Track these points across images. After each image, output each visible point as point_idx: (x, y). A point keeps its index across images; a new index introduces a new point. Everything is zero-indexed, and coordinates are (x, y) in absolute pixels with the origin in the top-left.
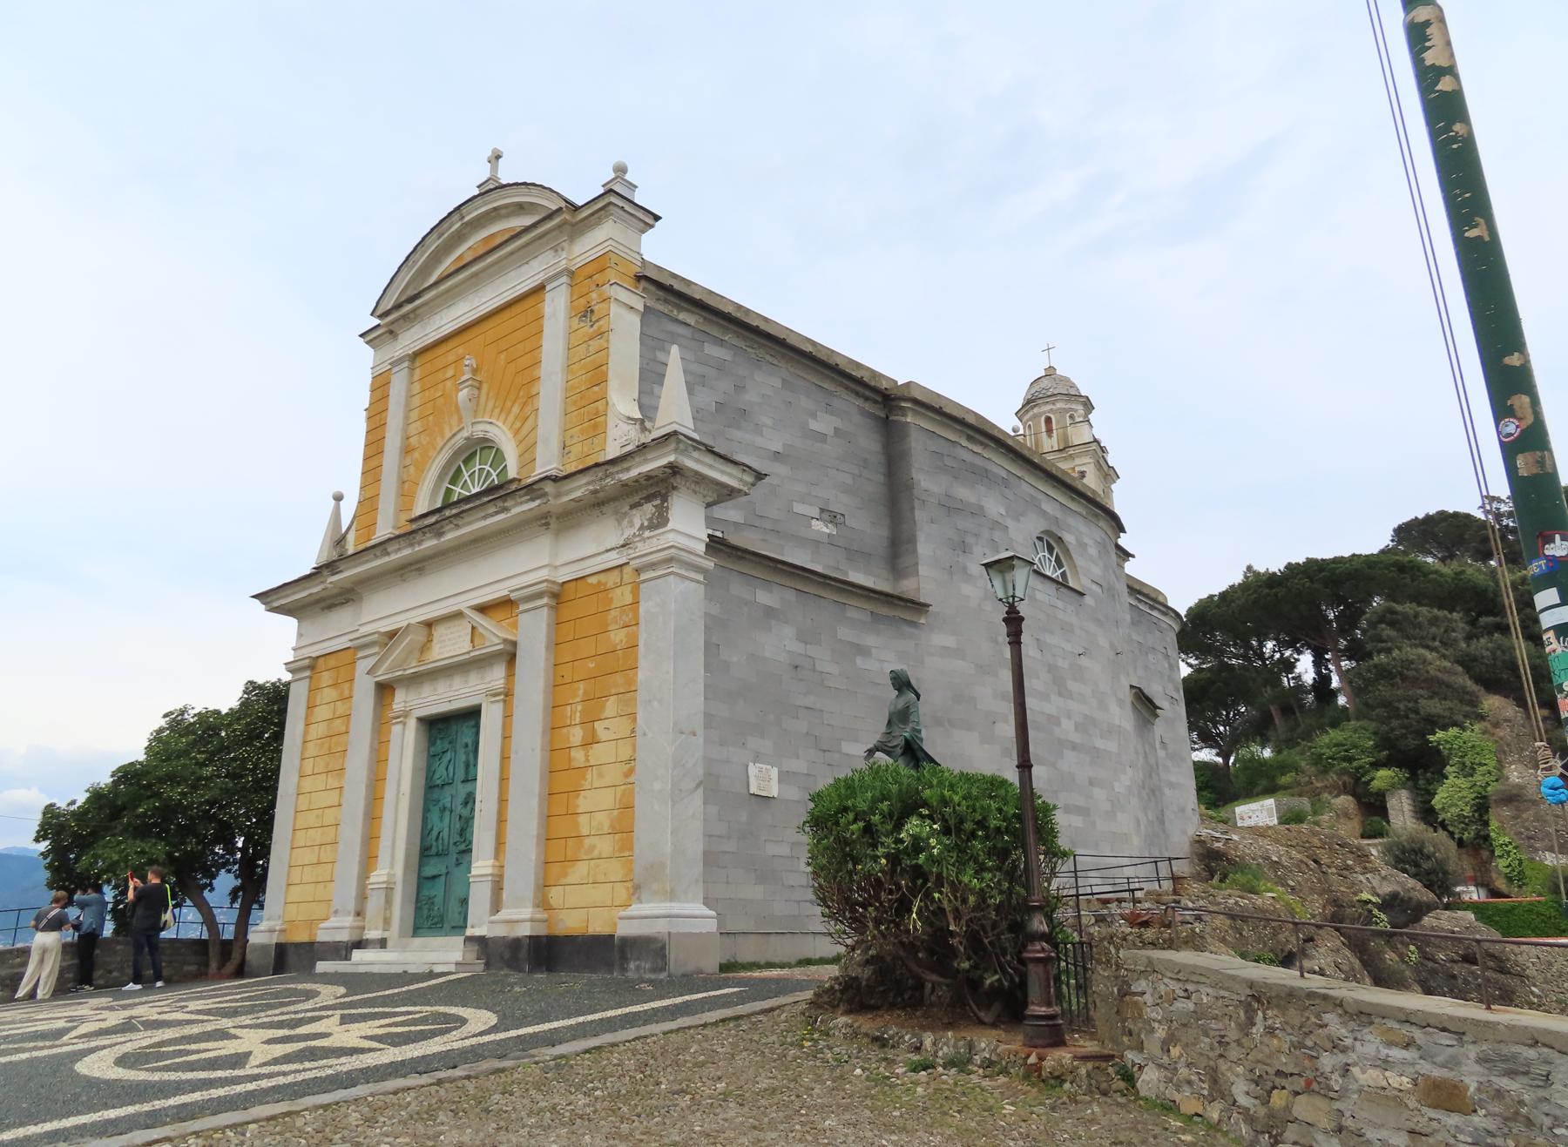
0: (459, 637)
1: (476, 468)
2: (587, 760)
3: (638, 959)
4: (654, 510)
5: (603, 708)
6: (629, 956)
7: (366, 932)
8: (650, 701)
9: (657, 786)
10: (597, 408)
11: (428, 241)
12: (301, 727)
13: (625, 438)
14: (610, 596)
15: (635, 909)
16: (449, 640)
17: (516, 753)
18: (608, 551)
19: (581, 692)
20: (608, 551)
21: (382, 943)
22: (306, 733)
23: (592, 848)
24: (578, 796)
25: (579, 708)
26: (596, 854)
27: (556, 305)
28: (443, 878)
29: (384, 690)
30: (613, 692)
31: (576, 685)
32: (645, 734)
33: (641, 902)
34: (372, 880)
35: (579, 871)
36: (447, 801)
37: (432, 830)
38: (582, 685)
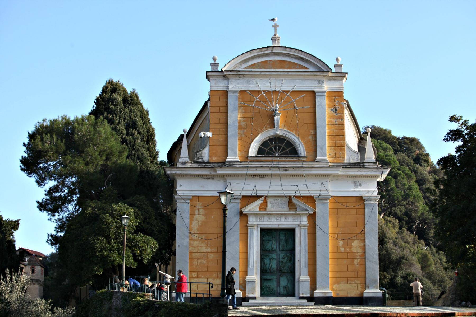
0: (282, 204)
7: (247, 295)
8: (370, 237)
11: (253, 51)
15: (367, 291)
16: (276, 204)
21: (255, 298)
22: (191, 224)
28: (274, 280)
29: (243, 216)
32: (369, 246)
33: (369, 289)
34: (247, 279)
36: (274, 256)
37: (266, 265)
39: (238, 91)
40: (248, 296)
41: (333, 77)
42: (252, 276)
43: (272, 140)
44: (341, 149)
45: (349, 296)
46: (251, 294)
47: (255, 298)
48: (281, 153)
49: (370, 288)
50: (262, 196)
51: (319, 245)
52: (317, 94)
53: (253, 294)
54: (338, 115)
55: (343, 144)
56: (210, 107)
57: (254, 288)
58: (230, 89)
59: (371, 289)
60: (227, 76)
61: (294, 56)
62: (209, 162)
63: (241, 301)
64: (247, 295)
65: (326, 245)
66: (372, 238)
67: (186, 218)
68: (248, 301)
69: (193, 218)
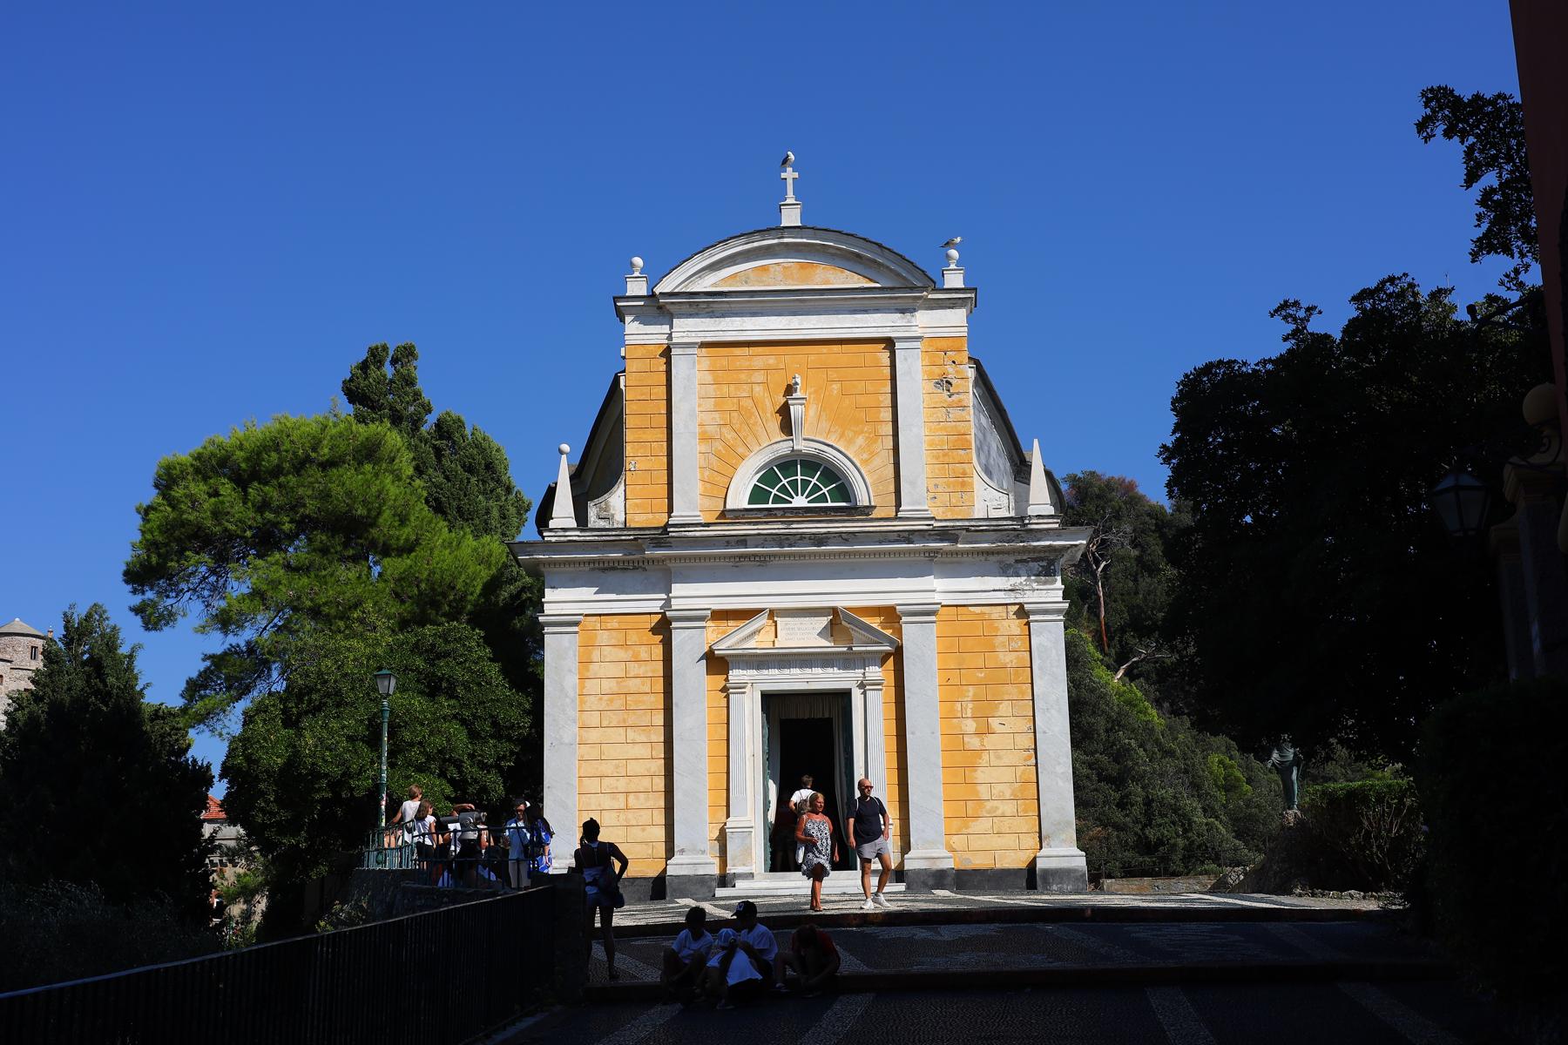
1: (814, 481)
2: (983, 745)
3: (1060, 883)
4: (1040, 569)
5: (997, 707)
6: (1051, 881)
7: (728, 867)
9: (1059, 769)
10: (964, 470)
12: (571, 681)
13: (995, 503)
14: (996, 625)
17: (913, 733)
18: (994, 590)
19: (971, 694)
20: (994, 590)
21: (751, 876)
23: (997, 808)
24: (976, 770)
25: (970, 705)
26: (999, 813)
27: (913, 368)
30: (1006, 698)
31: (965, 687)
32: (1045, 732)
35: (983, 825)
38: (971, 688)
39: (696, 343)
40: (733, 871)
41: (940, 302)
42: (742, 819)
43: (787, 464)
44: (963, 484)
45: (998, 866)
46: (740, 866)
47: (751, 876)
48: (809, 499)
49: (1052, 843)
50: (761, 610)
51: (913, 733)
52: (898, 345)
53: (744, 865)
54: (954, 397)
55: (968, 471)
56: (625, 386)
57: (748, 851)
58: (674, 341)
59: (1056, 847)
60: (668, 307)
61: (839, 252)
62: (626, 528)
63: (714, 884)
64: (730, 870)
65: (933, 733)
66: (1053, 711)
67: (570, 671)
68: (734, 886)
69: (588, 670)
